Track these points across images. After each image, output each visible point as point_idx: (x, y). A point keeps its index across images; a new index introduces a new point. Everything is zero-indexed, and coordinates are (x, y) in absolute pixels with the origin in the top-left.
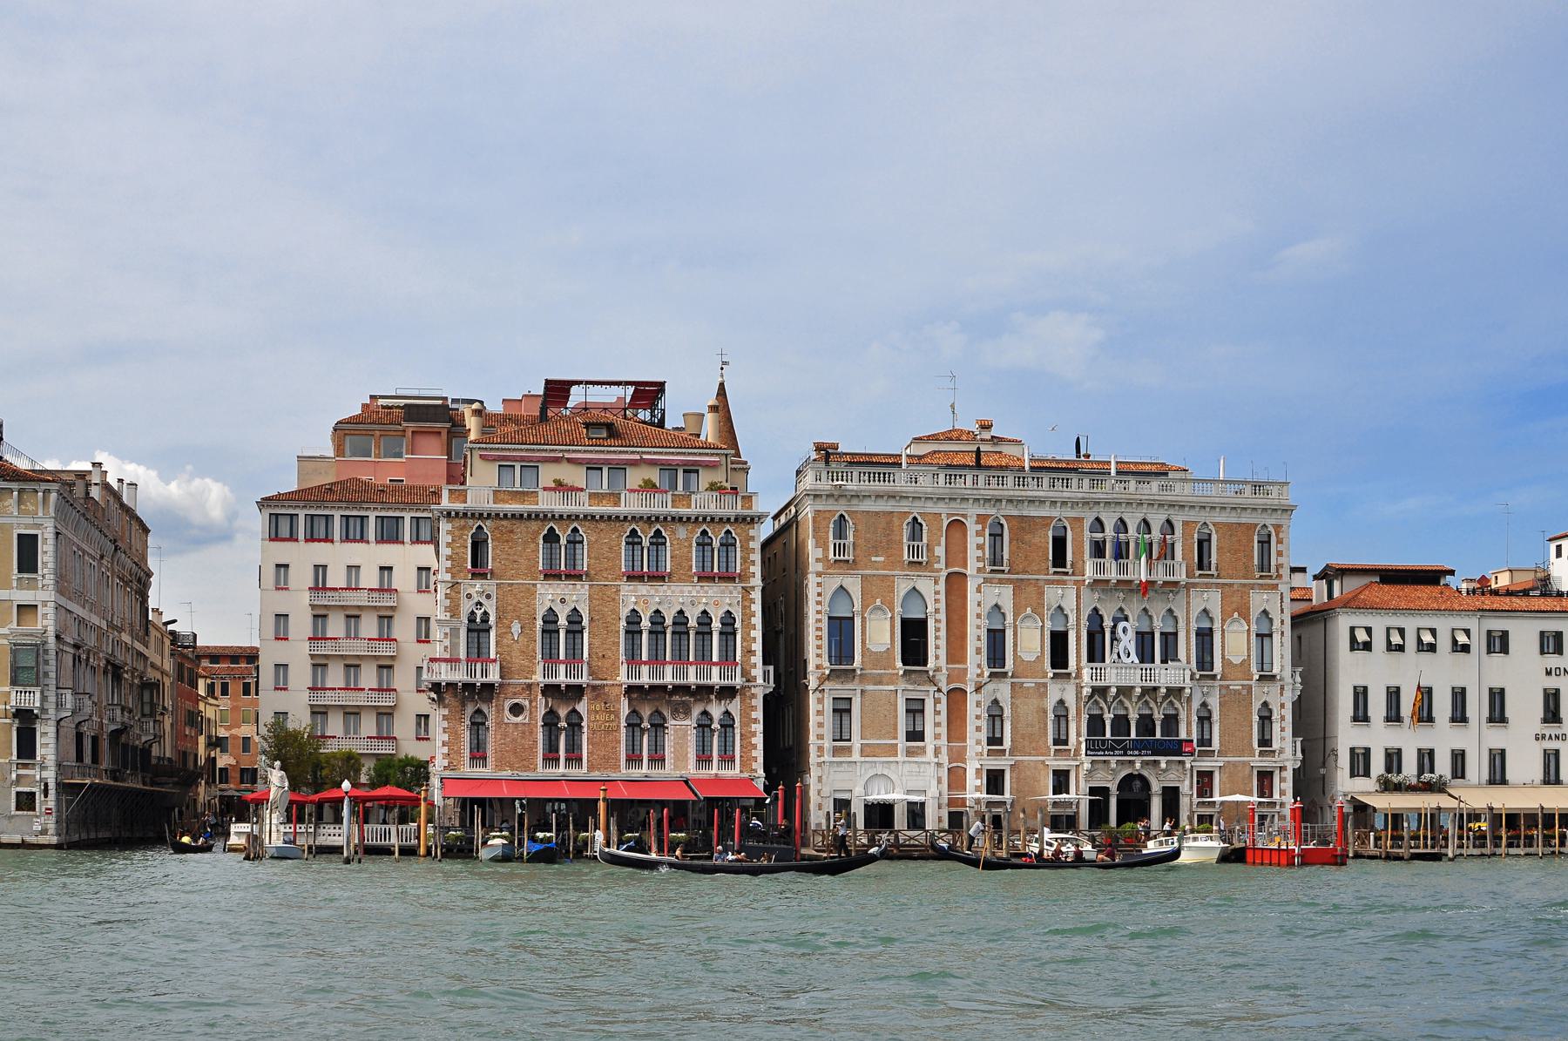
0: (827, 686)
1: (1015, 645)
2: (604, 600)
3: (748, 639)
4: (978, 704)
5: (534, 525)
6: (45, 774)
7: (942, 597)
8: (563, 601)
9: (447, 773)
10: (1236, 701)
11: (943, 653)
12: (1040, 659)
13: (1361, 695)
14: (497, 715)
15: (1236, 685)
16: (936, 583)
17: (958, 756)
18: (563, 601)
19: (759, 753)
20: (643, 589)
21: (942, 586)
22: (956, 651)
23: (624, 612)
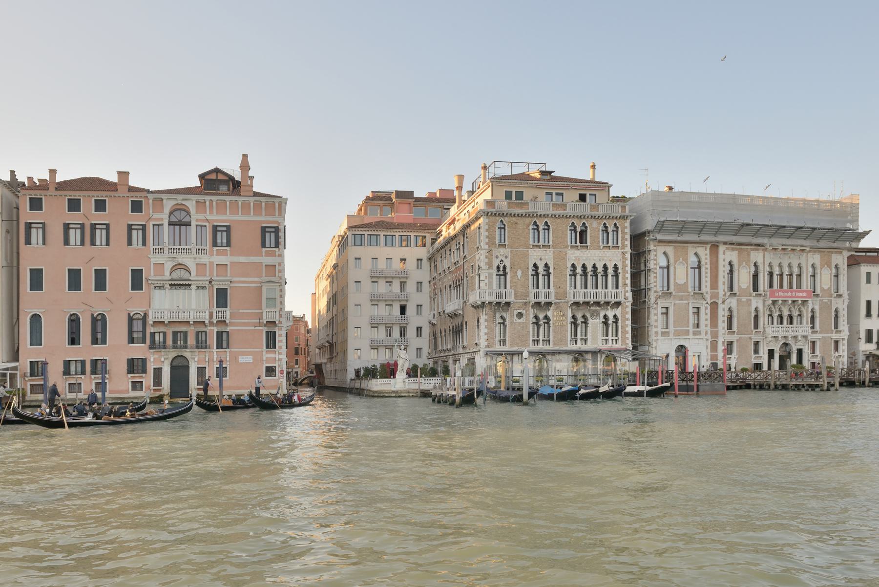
0: (659, 301)
2: (560, 258)
3: (624, 278)
4: (724, 309)
5: (528, 220)
6: (281, 357)
7: (708, 257)
8: (541, 259)
9: (488, 349)
10: (826, 307)
11: (708, 284)
14: (511, 317)
15: (826, 300)
17: (715, 335)
18: (541, 259)
19: (629, 335)
20: (577, 253)
21: (708, 252)
22: (714, 285)
23: (569, 266)
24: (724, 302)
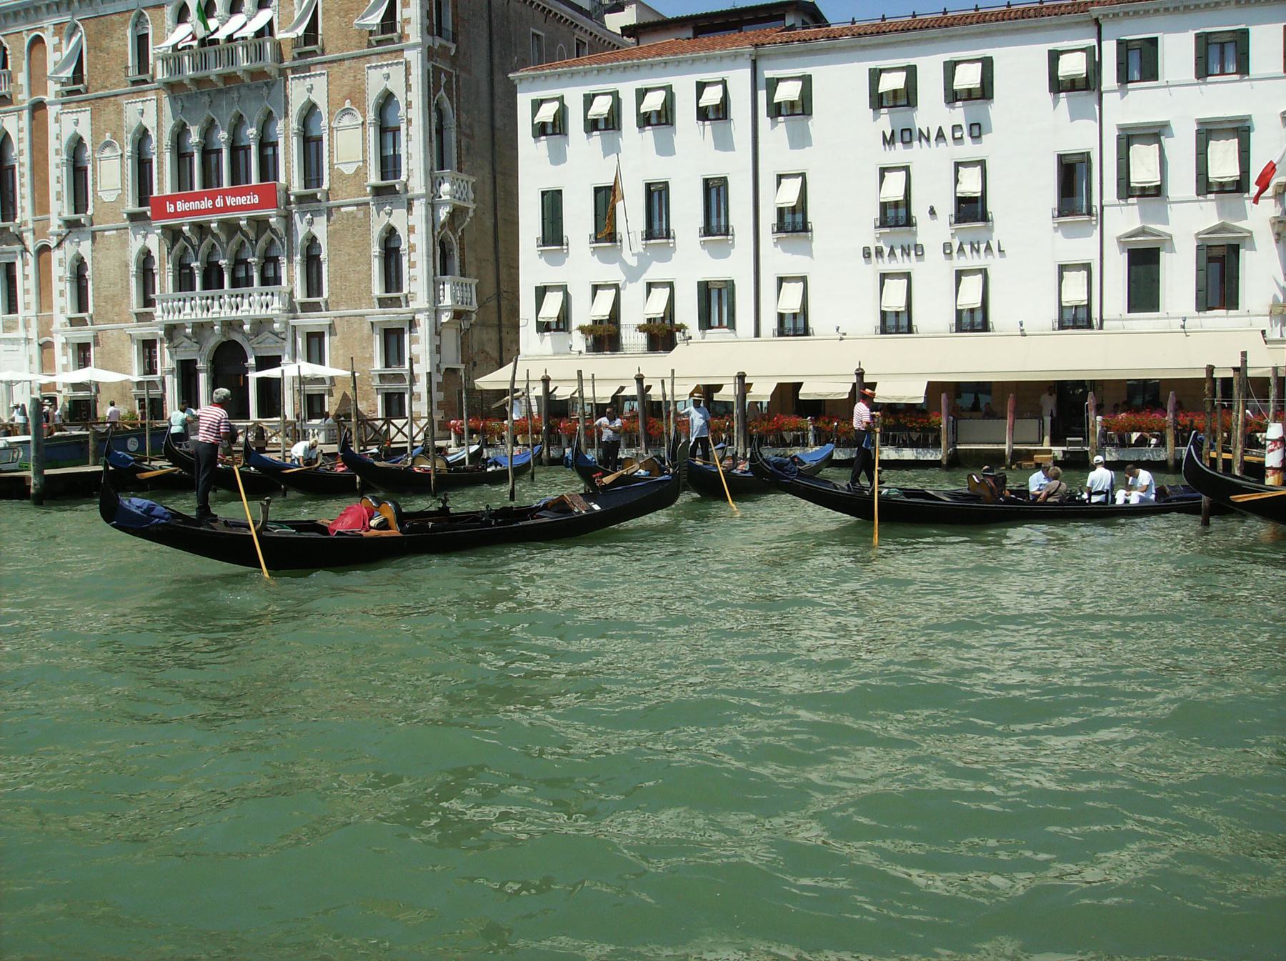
1: (95, 184)
7: (26, 135)
12: (121, 198)
13: (552, 202)
16: (20, 118)
24: (59, 245)
